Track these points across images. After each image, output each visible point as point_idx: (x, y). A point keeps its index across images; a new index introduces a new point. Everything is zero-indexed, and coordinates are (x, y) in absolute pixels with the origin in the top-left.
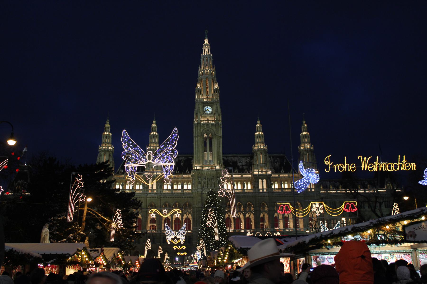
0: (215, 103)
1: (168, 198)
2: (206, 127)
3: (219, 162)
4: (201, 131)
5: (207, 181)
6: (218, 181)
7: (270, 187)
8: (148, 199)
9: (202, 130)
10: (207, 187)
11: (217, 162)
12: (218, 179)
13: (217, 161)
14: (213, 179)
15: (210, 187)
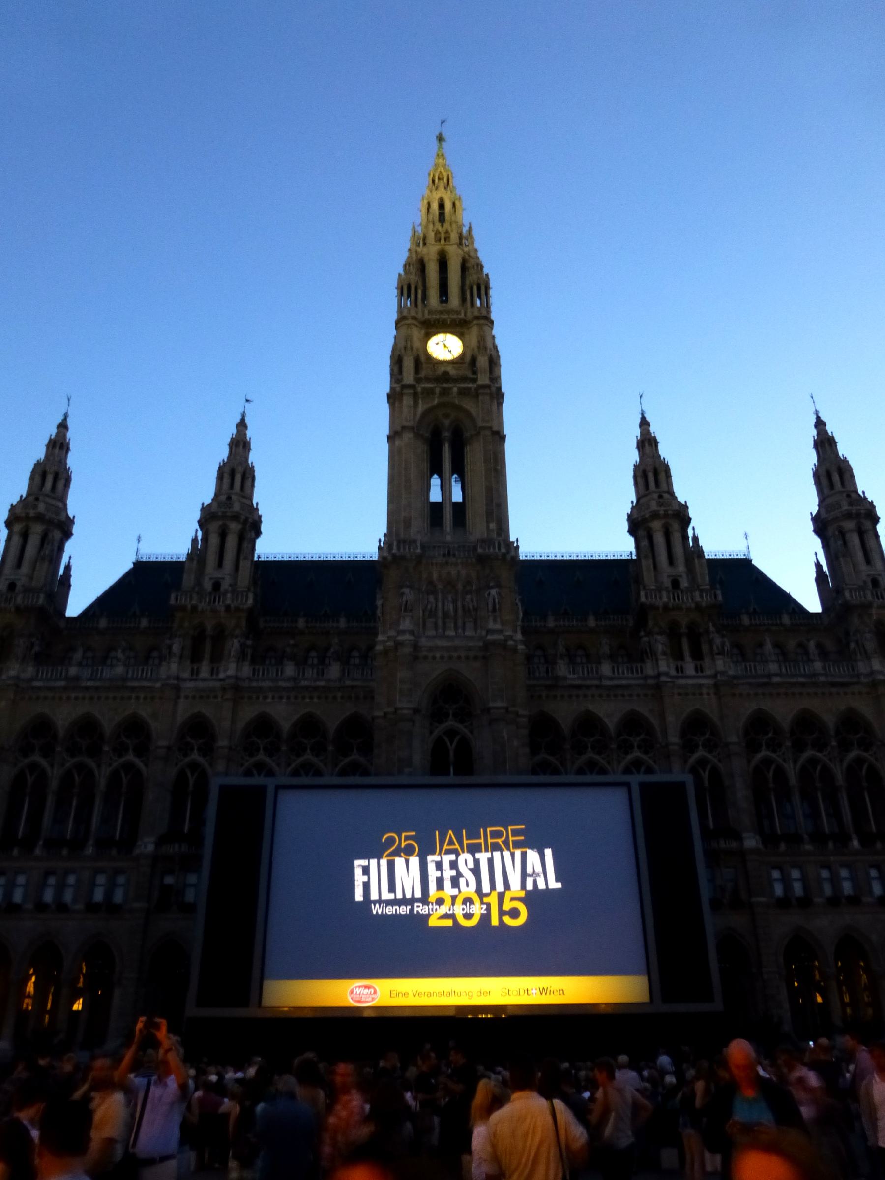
0: (475, 322)
1: (269, 700)
2: (436, 402)
3: (493, 526)
4: (415, 414)
5: (440, 605)
6: (490, 602)
7: (718, 654)
8: (182, 700)
9: (420, 409)
10: (440, 631)
11: (488, 527)
12: (494, 592)
13: (488, 522)
14: (469, 597)
15: (456, 628)
